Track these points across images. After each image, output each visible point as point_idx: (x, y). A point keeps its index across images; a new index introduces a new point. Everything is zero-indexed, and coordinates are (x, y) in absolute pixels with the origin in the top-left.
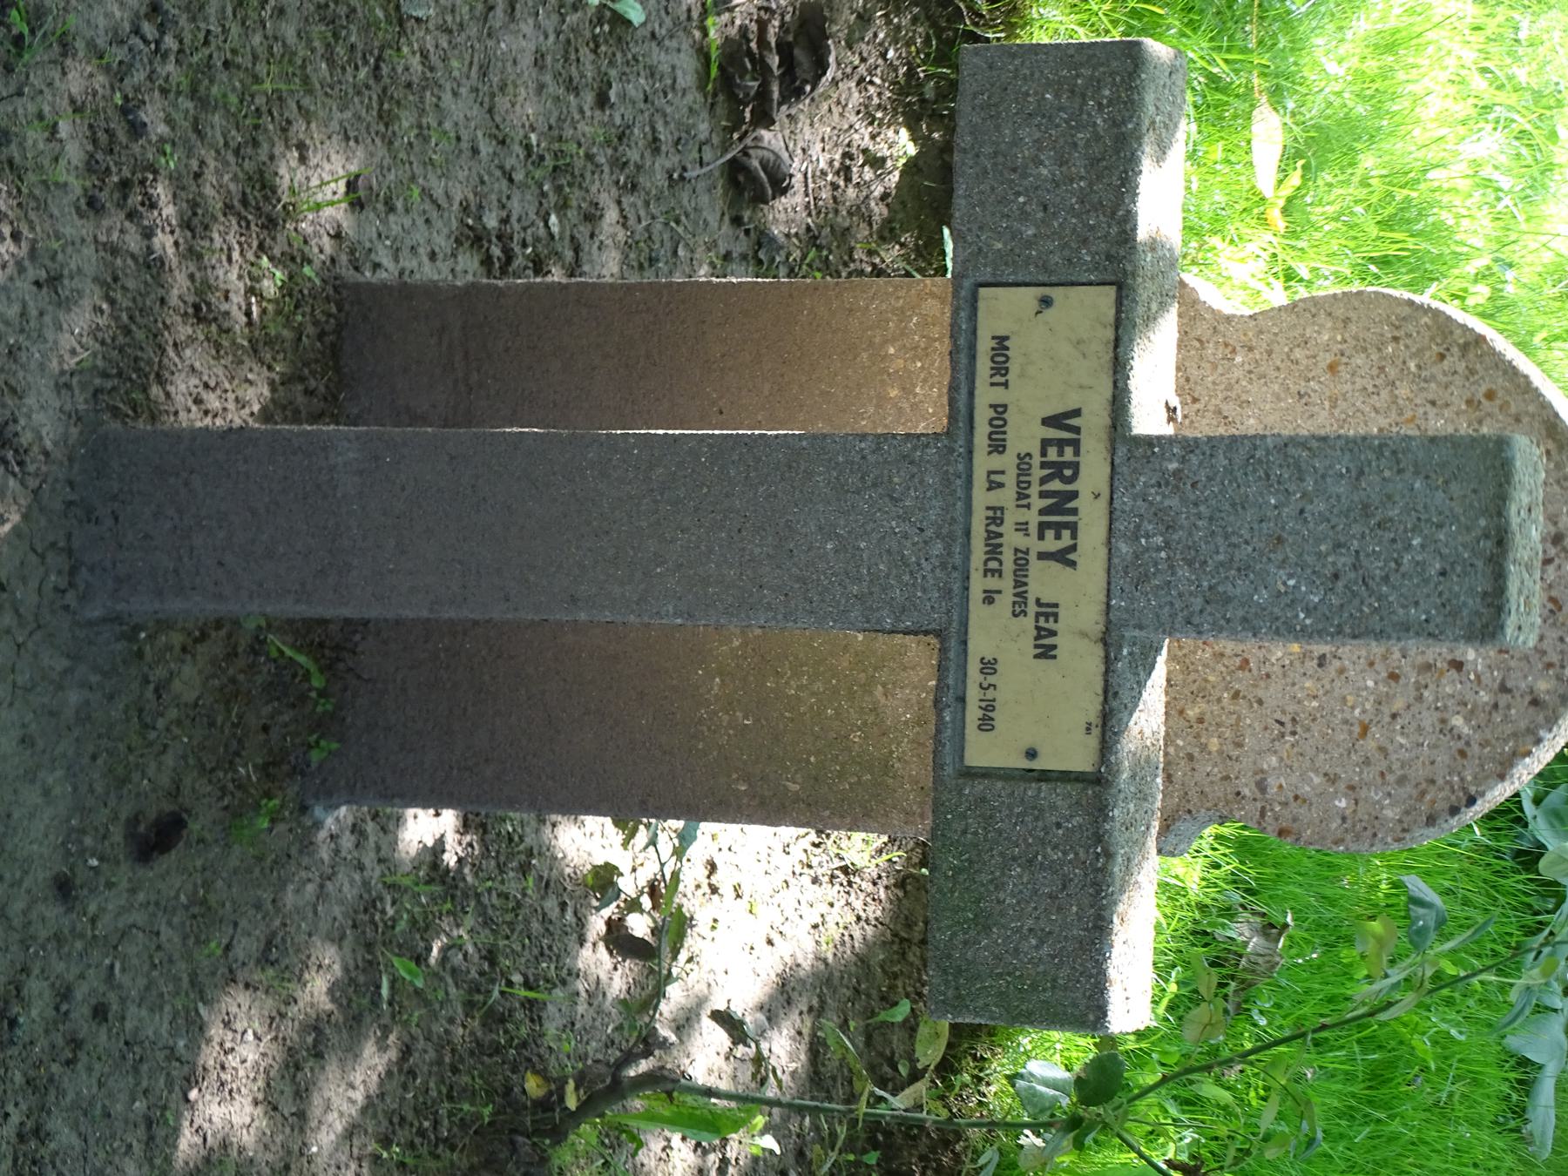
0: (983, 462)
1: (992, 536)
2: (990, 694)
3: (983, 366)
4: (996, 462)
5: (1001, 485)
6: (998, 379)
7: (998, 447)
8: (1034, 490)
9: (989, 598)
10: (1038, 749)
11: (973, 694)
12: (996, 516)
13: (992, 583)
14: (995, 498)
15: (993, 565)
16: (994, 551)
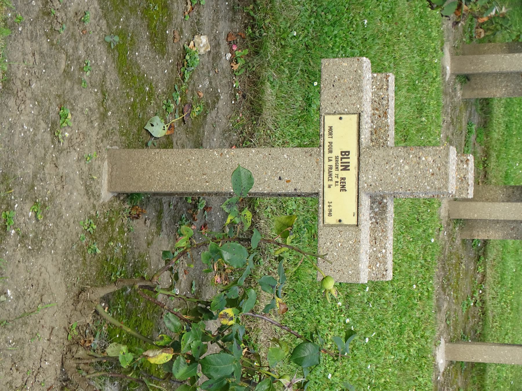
0: (327, 155)
1: (329, 172)
2: (331, 208)
3: (326, 133)
4: (330, 155)
5: (331, 160)
6: (330, 136)
7: (330, 151)
8: (340, 162)
9: (329, 187)
10: (342, 219)
11: (326, 208)
12: (331, 167)
13: (330, 183)
14: (331, 163)
15: (330, 178)
16: (330, 175)
